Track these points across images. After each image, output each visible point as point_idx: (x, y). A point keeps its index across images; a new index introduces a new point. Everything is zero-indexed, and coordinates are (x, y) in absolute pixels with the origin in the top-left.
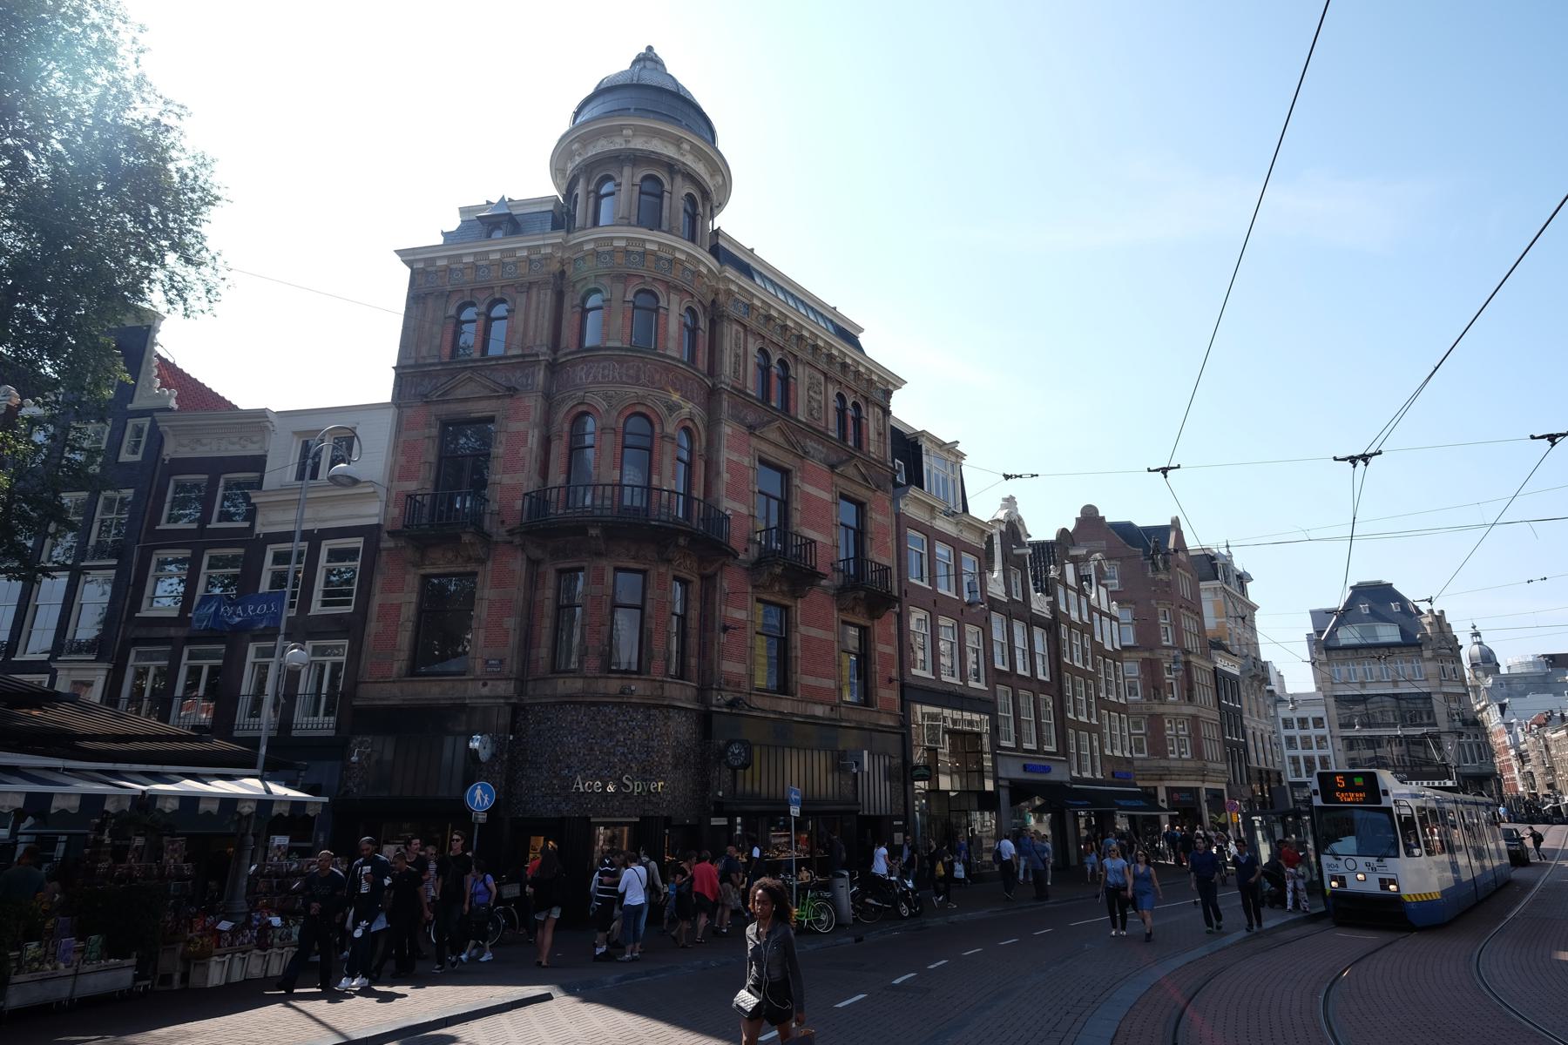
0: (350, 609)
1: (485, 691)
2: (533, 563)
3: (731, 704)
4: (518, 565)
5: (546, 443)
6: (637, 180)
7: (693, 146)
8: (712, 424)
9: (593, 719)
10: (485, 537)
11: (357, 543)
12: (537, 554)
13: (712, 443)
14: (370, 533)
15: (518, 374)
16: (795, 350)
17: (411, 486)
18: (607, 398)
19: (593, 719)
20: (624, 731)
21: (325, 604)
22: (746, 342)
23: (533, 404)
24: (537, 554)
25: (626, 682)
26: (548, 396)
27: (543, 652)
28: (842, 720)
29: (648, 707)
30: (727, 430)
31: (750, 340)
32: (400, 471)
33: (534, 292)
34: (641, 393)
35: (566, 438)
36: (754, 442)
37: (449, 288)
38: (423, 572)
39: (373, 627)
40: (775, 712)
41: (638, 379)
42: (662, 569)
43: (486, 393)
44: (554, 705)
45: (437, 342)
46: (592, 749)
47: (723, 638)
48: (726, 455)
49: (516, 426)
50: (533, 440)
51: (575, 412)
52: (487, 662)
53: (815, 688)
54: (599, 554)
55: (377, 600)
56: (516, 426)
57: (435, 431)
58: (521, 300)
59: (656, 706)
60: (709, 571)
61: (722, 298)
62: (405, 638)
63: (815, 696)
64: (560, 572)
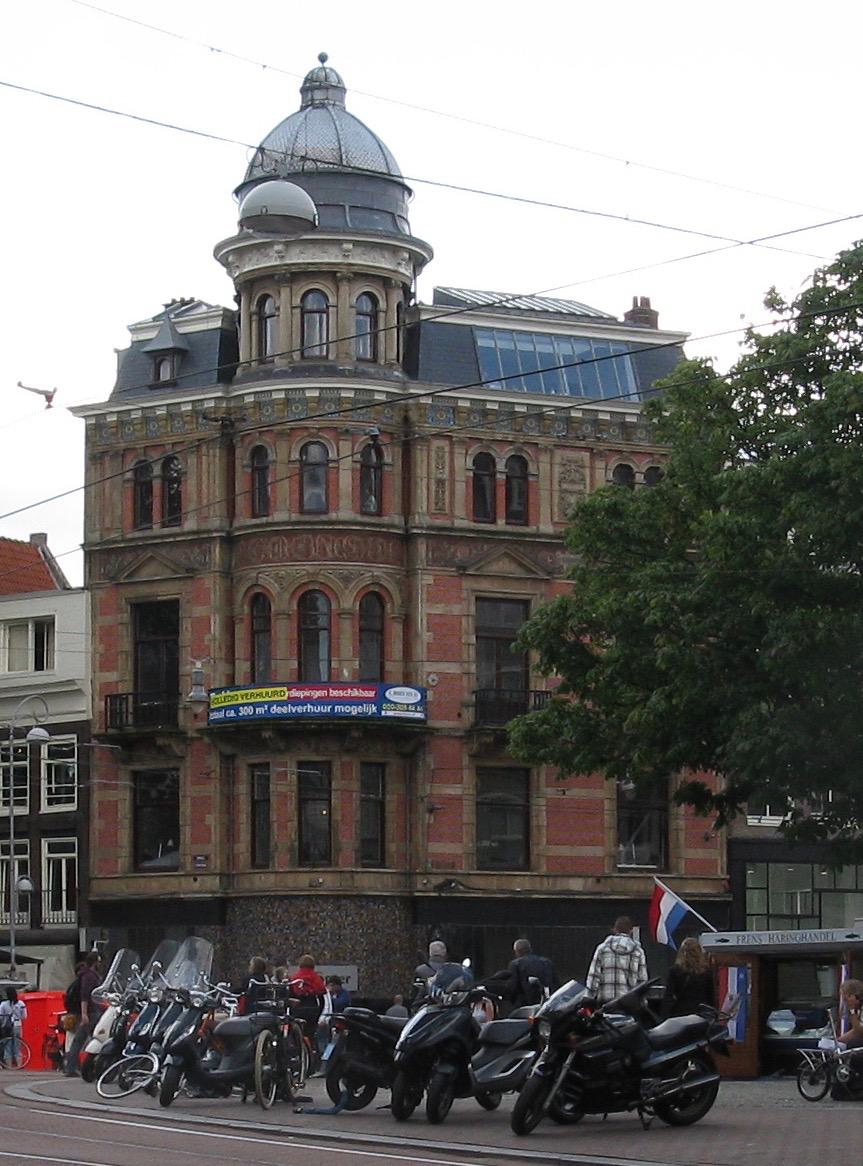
0: (72, 807)
1: (196, 885)
2: (228, 760)
3: (439, 888)
4: (213, 762)
5: (230, 626)
6: (297, 301)
7: (356, 243)
8: (408, 576)
9: (287, 911)
10: (180, 735)
11: (73, 738)
12: (228, 750)
13: (409, 600)
14: (80, 728)
15: (197, 550)
16: (533, 435)
17: (113, 676)
18: (279, 579)
19: (287, 911)
20: (315, 921)
21: (50, 802)
22: (452, 453)
23: (212, 584)
24: (228, 750)
25: (313, 876)
26: (227, 574)
27: (243, 846)
28: (613, 893)
29: (338, 898)
30: (425, 580)
31: (459, 450)
32: (103, 662)
33: (204, 449)
34: (311, 569)
35: (247, 622)
36: (467, 584)
37: (123, 445)
38: (131, 768)
39: (97, 824)
40: (502, 891)
41: (308, 552)
42: (346, 758)
43: (168, 574)
44: (254, 897)
45: (118, 512)
46: (287, 939)
47: (429, 819)
48: (423, 611)
49: (199, 611)
50: (216, 627)
51: (252, 593)
52: (195, 858)
53: (571, 858)
54: (280, 752)
55: (96, 797)
56: (199, 611)
57: (126, 617)
58: (192, 460)
59: (345, 897)
60: (408, 749)
61: (413, 416)
62: (125, 836)
63: (566, 868)
64: (253, 766)
